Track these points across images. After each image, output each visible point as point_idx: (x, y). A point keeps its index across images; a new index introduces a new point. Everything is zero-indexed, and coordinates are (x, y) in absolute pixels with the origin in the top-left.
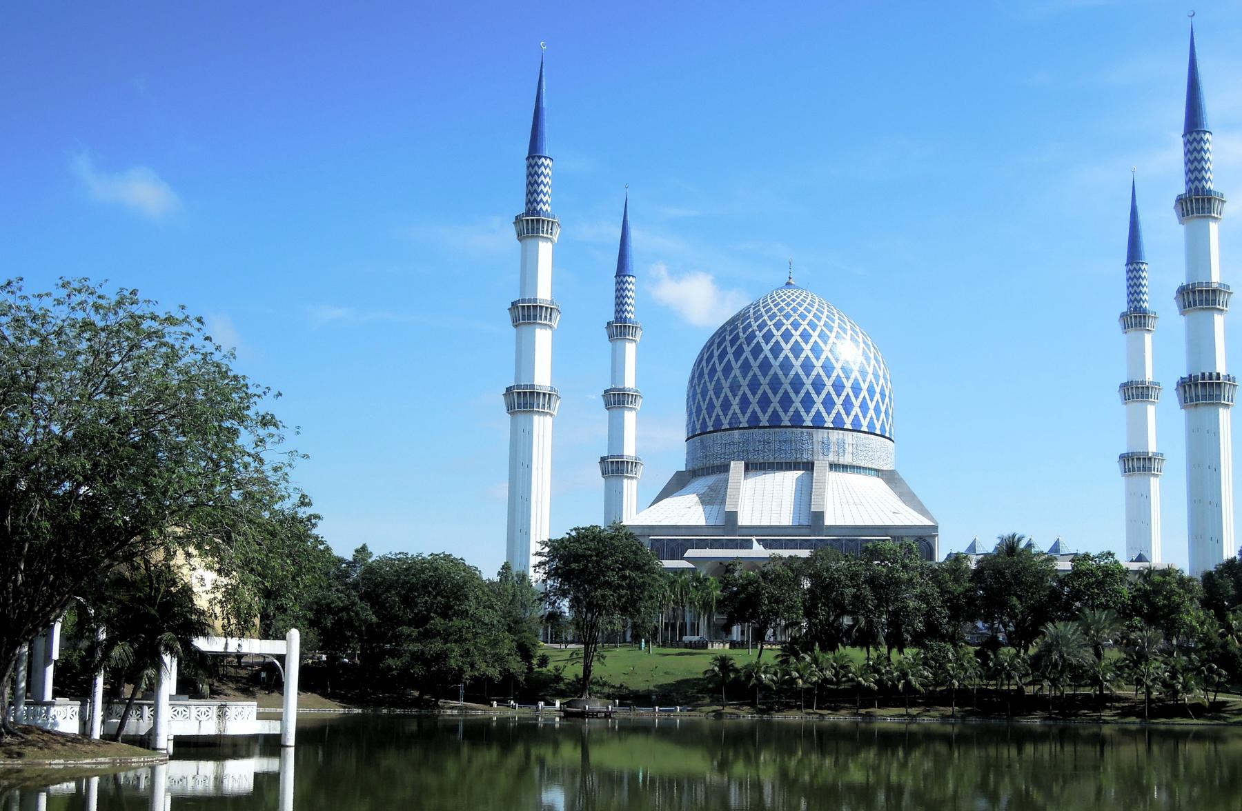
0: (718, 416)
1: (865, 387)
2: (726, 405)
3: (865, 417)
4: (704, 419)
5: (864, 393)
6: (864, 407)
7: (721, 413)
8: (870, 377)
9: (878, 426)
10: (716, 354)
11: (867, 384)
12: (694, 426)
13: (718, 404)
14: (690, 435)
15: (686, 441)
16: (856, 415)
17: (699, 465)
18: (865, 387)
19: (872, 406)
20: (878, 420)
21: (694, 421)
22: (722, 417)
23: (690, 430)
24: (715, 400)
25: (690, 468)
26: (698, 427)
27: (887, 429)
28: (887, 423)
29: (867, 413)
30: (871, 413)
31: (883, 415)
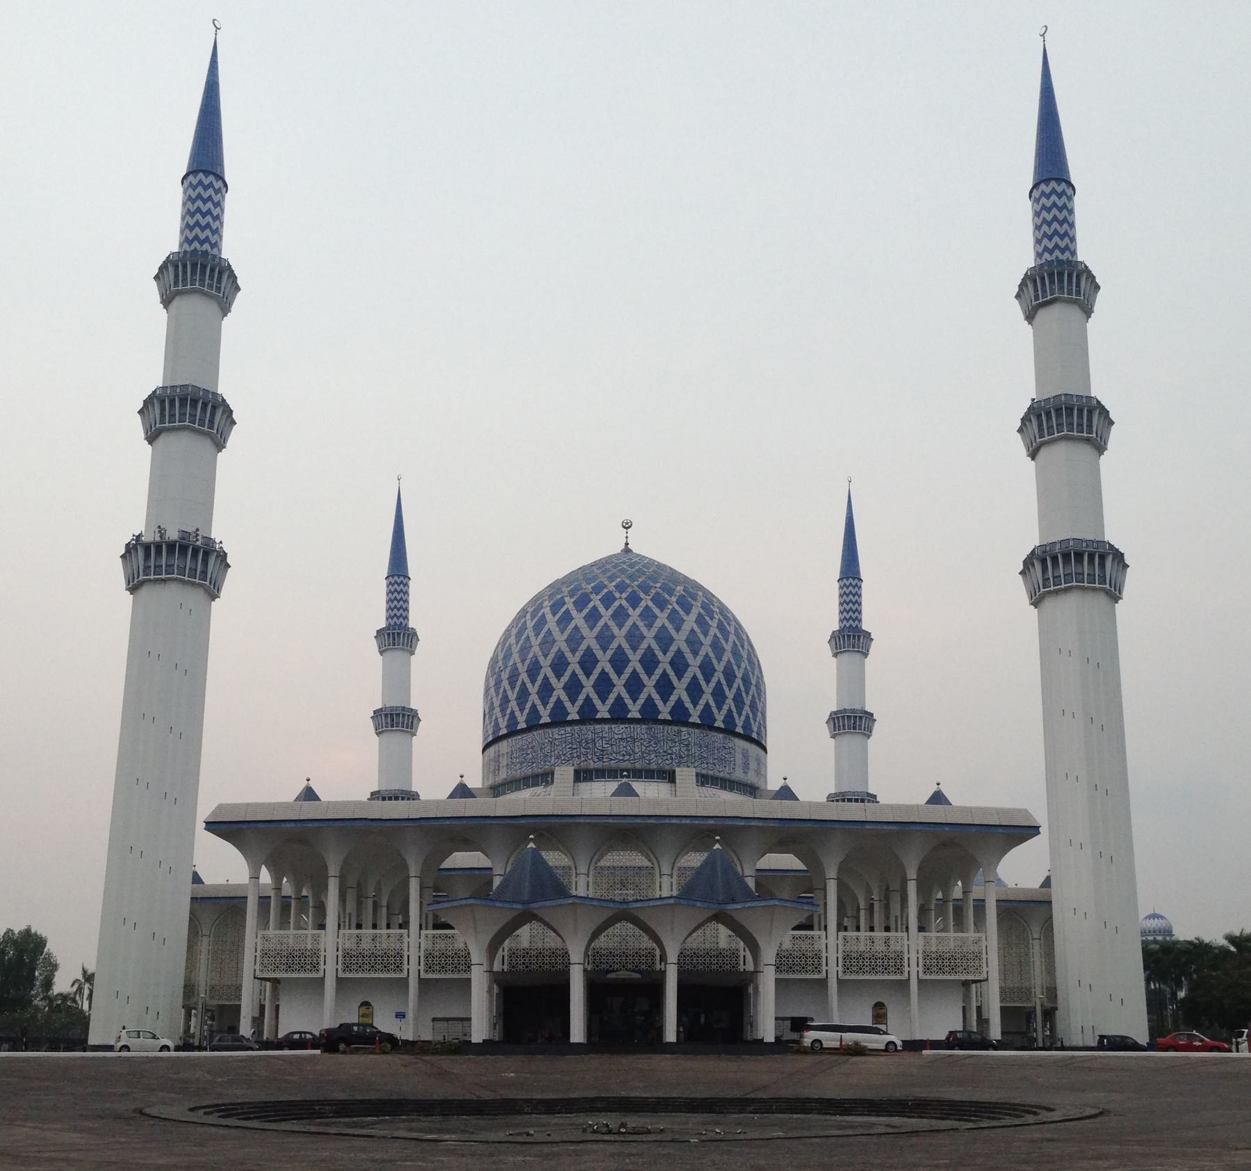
0: (534, 706)
1: (720, 667)
2: (546, 690)
3: (719, 709)
4: (513, 713)
5: (719, 676)
6: (719, 695)
7: (538, 702)
8: (727, 656)
9: (740, 722)
10: (530, 624)
11: (723, 664)
12: (497, 724)
13: (533, 689)
14: (490, 738)
15: (484, 751)
16: (707, 705)
17: (503, 775)
18: (720, 667)
19: (730, 694)
20: (740, 714)
21: (496, 719)
22: (540, 708)
23: (490, 732)
24: (529, 685)
25: (490, 782)
26: (503, 724)
27: (755, 729)
28: (755, 720)
29: (724, 703)
30: (729, 703)
31: (747, 709)
